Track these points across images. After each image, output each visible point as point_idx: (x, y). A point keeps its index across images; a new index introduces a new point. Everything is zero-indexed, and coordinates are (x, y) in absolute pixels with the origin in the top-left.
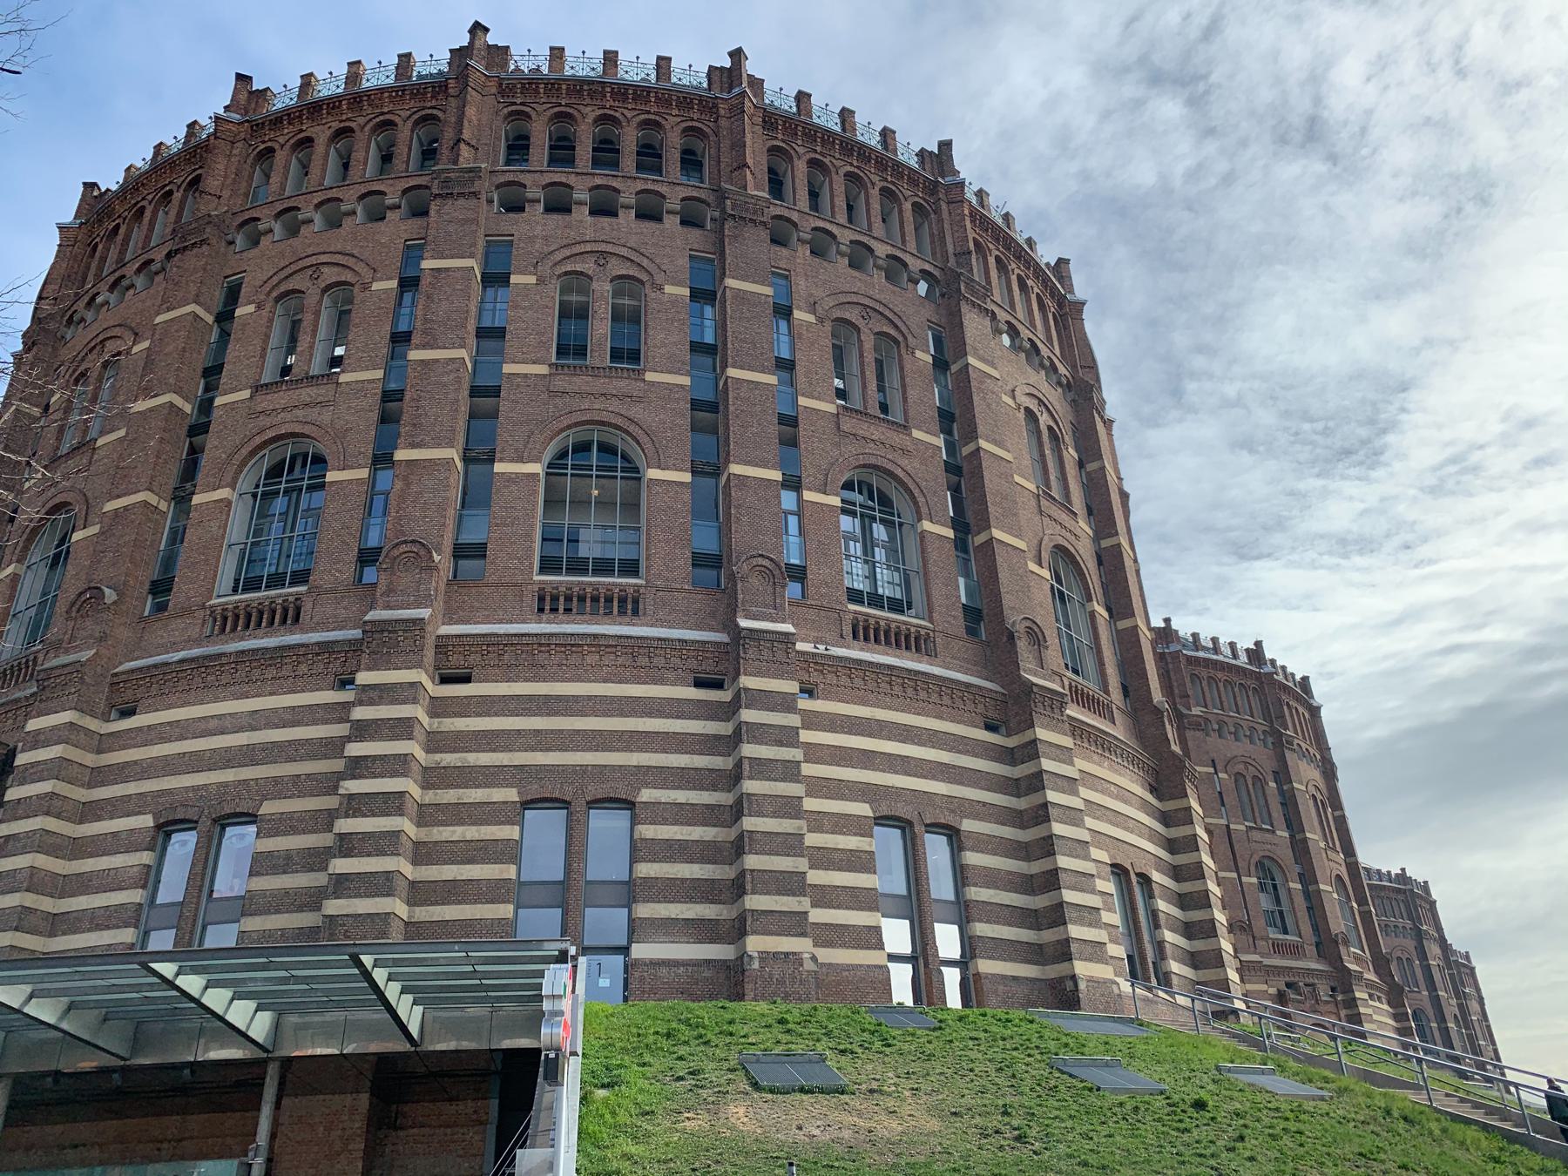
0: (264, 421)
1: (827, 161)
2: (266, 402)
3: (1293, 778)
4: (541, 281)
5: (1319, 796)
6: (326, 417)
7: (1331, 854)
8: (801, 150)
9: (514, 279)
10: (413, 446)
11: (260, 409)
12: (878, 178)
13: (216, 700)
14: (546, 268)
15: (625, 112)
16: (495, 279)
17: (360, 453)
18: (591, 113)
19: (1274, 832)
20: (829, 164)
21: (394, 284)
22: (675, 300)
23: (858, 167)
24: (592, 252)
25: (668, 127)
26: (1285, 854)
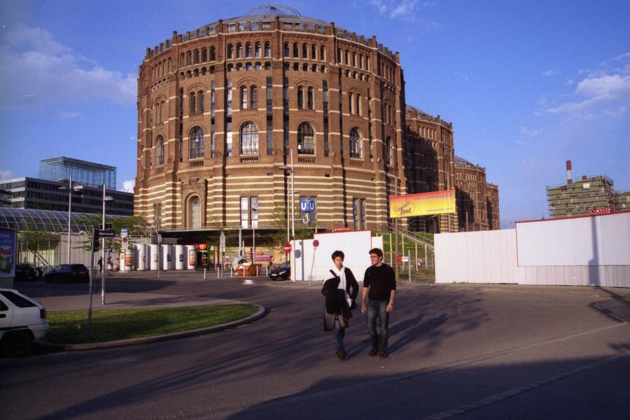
2: (243, 113)
4: (295, 88)
6: (256, 118)
10: (277, 129)
13: (247, 175)
18: (302, 42)
21: (265, 87)
22: (320, 92)
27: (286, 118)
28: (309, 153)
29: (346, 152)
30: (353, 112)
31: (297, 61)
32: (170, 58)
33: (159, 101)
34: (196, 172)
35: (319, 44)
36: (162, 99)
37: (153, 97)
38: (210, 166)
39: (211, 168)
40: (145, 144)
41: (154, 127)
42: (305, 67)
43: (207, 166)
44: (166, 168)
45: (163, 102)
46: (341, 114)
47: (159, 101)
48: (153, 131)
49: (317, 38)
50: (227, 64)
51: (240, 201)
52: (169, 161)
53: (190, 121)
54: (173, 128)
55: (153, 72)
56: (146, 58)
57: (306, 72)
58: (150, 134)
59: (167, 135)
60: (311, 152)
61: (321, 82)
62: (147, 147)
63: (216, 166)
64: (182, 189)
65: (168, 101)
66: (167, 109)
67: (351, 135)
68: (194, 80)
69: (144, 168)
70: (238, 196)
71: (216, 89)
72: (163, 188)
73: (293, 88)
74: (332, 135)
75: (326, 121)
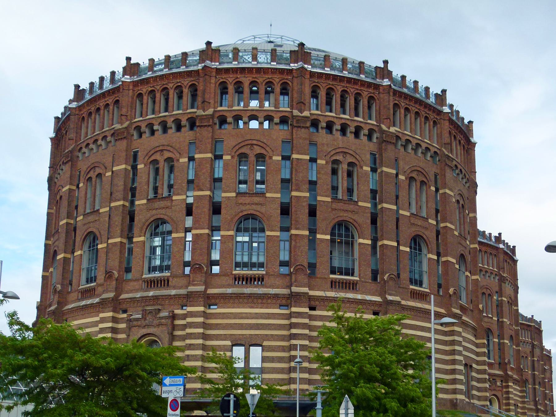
0: (243, 208)
1: (410, 108)
3: (503, 295)
4: (327, 162)
5: (510, 302)
6: (263, 210)
7: (511, 327)
8: (403, 104)
9: (319, 161)
11: (240, 202)
12: (424, 113)
14: (328, 158)
15: (351, 89)
16: (313, 160)
17: (276, 226)
19: (492, 318)
20: (410, 109)
23: (419, 109)
24: (342, 152)
25: (364, 96)
26: (495, 327)
27: (312, 212)
28: (347, 274)
29: (405, 276)
30: (414, 211)
31: (332, 119)
32: (118, 101)
33: (92, 174)
34: (156, 298)
35: (365, 94)
36: (98, 171)
37: (83, 166)
38: (180, 288)
39: (183, 292)
40: (61, 244)
41: (80, 218)
42: (343, 130)
43: (174, 288)
44: (100, 289)
45: (99, 175)
46: (397, 211)
47: (92, 174)
48: (79, 224)
49: (363, 83)
50: (217, 115)
51: (231, 351)
52: (109, 275)
53: (149, 210)
54: (117, 219)
55: (84, 126)
56: (71, 101)
57: (345, 138)
58: (72, 229)
59: (104, 233)
60: (349, 272)
61: (368, 156)
62: (65, 252)
63: (192, 288)
64: (130, 328)
65: (109, 174)
66: (107, 187)
67: (411, 248)
68: (160, 139)
69: (59, 287)
70: (229, 343)
71: (197, 156)
72: (95, 324)
73: (324, 162)
74: (382, 246)
75: (374, 221)
